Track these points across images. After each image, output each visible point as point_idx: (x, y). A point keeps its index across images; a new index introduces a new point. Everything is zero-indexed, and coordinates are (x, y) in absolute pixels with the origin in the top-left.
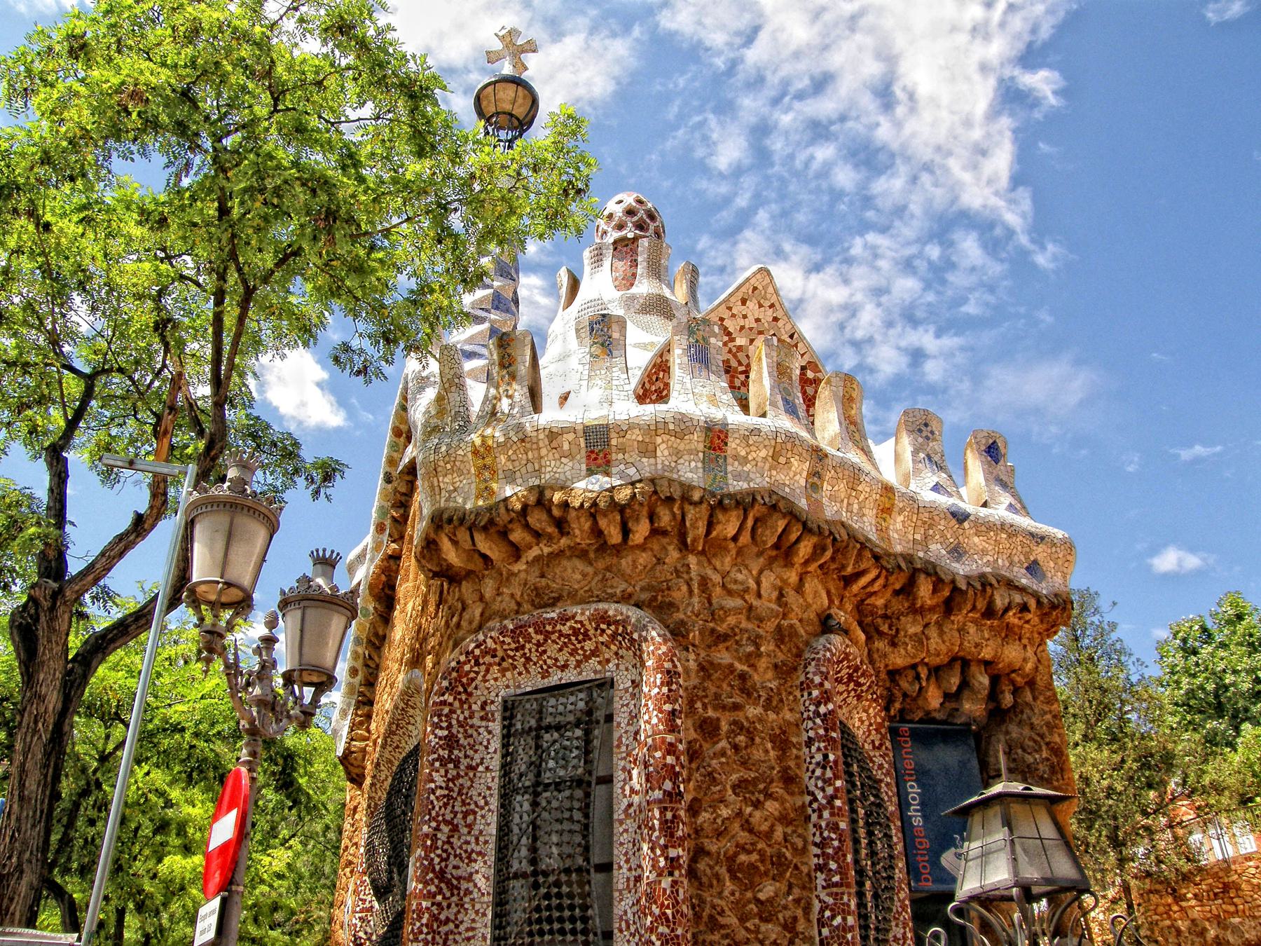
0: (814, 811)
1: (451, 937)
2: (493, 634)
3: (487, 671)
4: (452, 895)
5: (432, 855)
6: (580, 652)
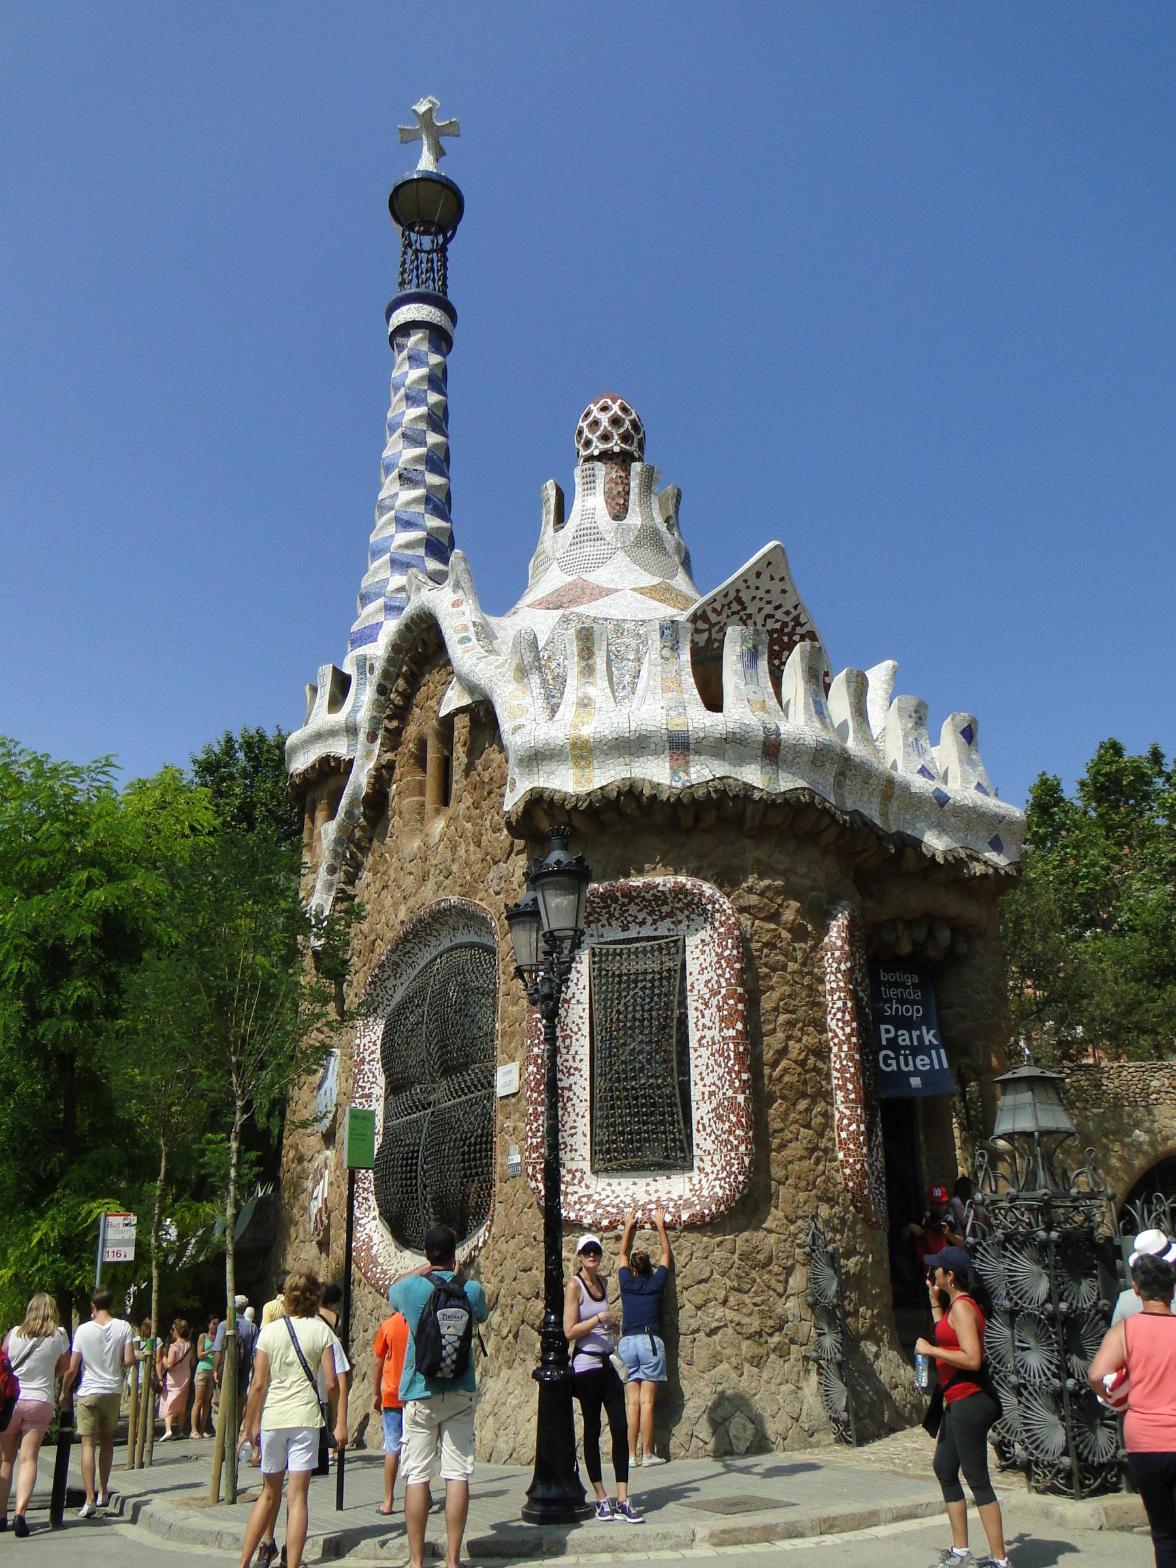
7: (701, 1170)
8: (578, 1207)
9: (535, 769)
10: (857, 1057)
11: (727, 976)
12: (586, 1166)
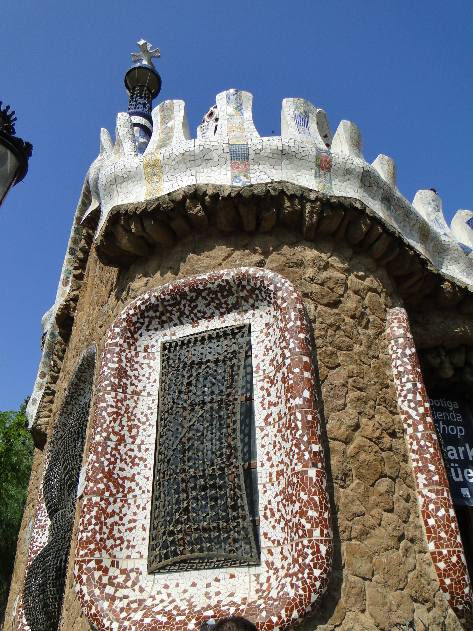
0: (409, 426)
1: (116, 528)
2: (156, 294)
3: (150, 323)
4: (118, 492)
5: (103, 459)
6: (224, 306)
7: (270, 565)
8: (124, 615)
9: (115, 193)
10: (435, 437)
11: (292, 346)
12: (143, 564)
